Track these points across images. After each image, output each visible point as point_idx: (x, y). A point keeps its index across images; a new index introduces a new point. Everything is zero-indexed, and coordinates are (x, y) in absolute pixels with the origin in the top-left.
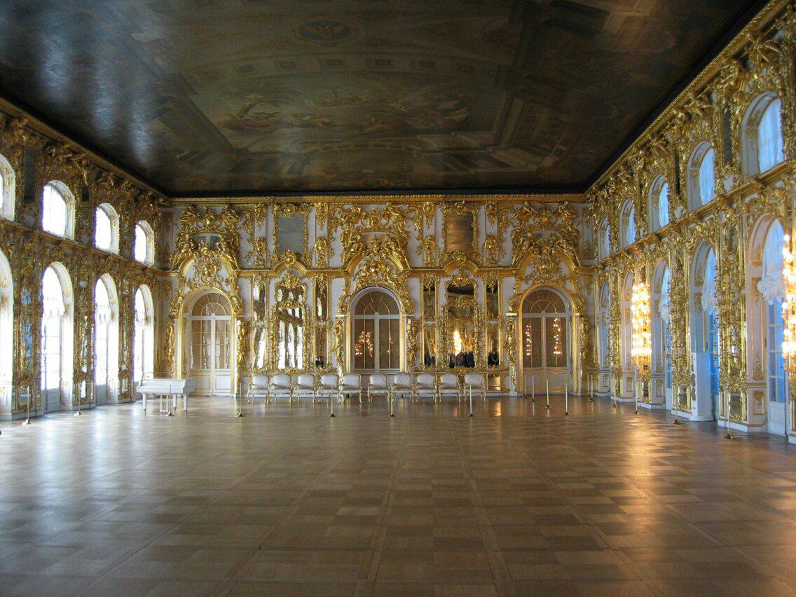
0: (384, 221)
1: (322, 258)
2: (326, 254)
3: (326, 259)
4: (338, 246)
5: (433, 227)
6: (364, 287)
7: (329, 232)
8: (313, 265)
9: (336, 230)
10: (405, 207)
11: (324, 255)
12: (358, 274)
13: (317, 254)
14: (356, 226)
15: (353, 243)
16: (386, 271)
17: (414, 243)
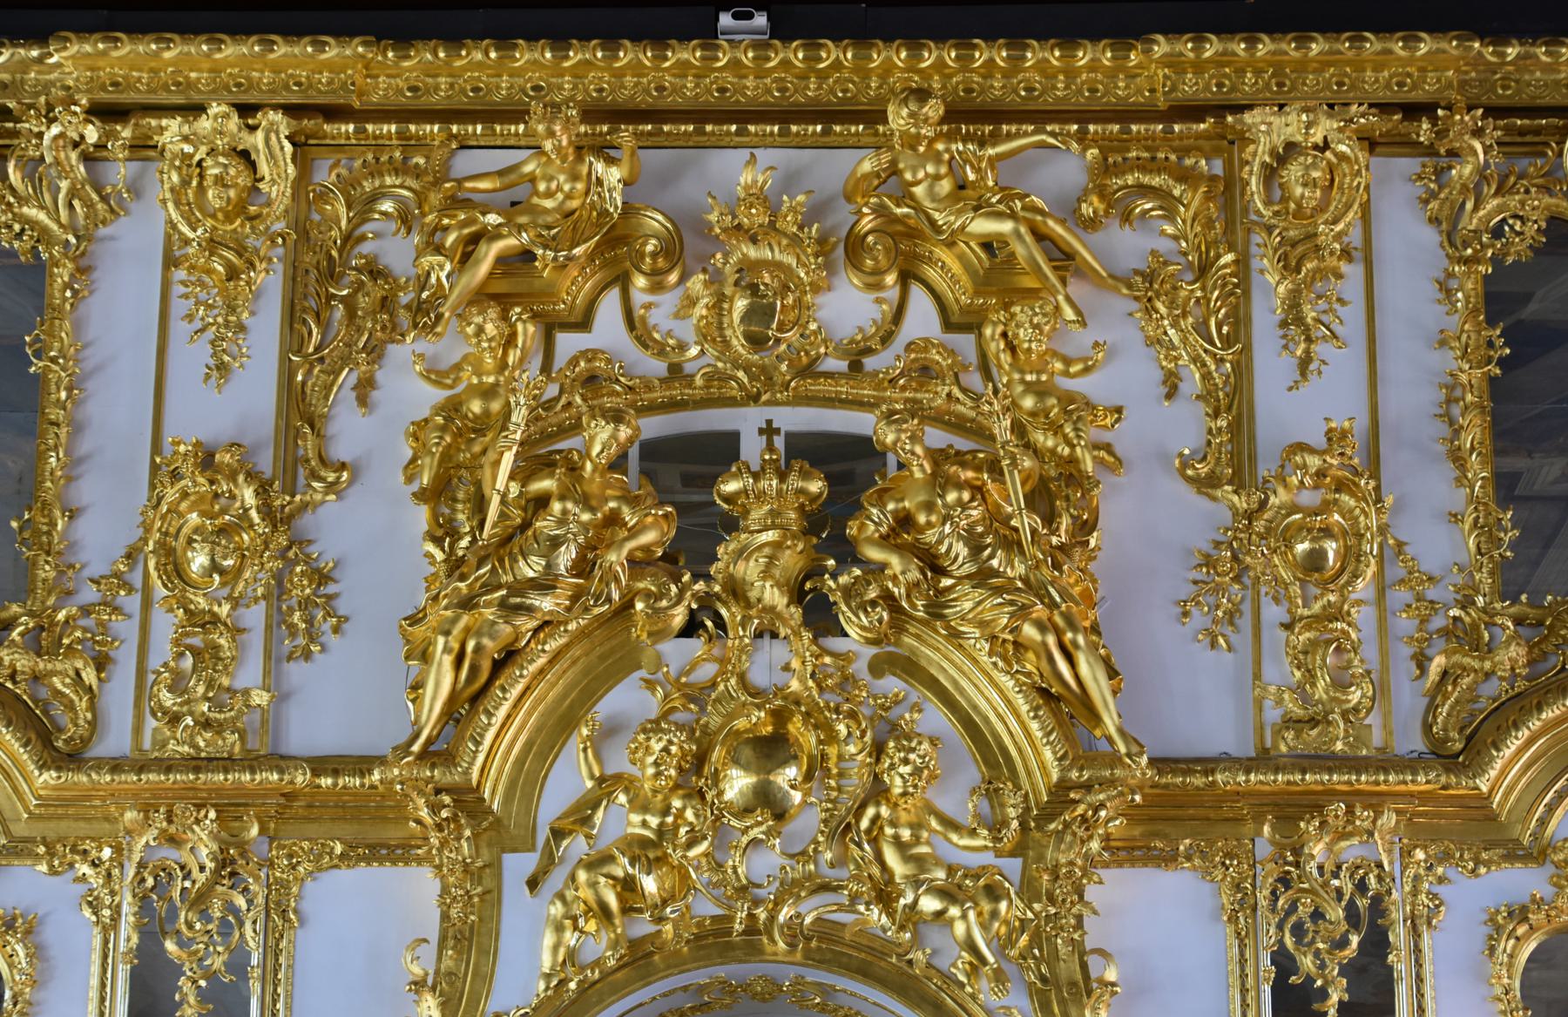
0: (848, 306)
1: (207, 656)
2: (255, 616)
3: (249, 674)
4: (377, 535)
5: (1341, 365)
6: (640, 959)
7: (299, 411)
8: (116, 740)
9: (364, 389)
10: (1064, 167)
11: (236, 631)
12: (581, 815)
13: (166, 624)
14: (568, 343)
15: (541, 503)
16: (878, 791)
17: (1150, 518)
